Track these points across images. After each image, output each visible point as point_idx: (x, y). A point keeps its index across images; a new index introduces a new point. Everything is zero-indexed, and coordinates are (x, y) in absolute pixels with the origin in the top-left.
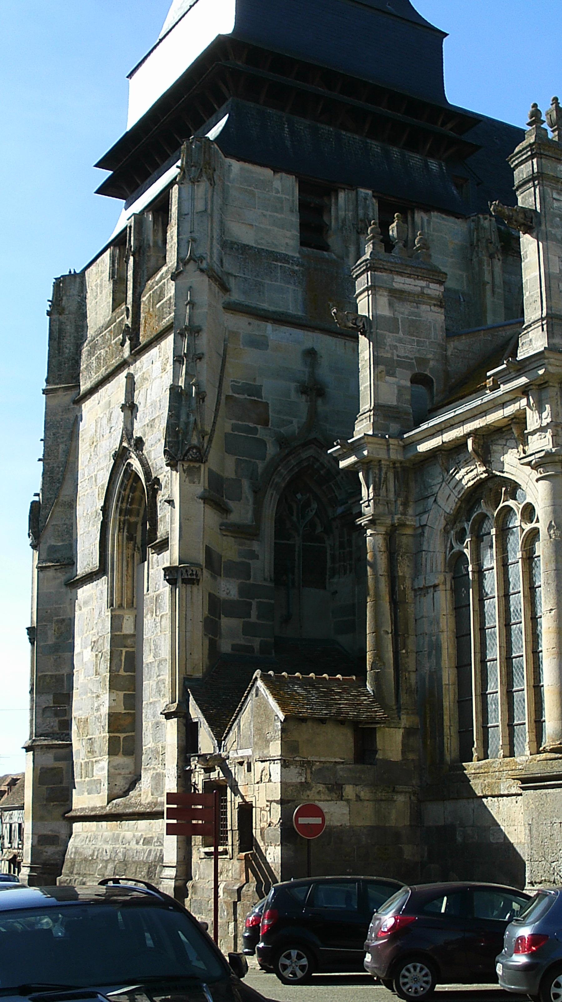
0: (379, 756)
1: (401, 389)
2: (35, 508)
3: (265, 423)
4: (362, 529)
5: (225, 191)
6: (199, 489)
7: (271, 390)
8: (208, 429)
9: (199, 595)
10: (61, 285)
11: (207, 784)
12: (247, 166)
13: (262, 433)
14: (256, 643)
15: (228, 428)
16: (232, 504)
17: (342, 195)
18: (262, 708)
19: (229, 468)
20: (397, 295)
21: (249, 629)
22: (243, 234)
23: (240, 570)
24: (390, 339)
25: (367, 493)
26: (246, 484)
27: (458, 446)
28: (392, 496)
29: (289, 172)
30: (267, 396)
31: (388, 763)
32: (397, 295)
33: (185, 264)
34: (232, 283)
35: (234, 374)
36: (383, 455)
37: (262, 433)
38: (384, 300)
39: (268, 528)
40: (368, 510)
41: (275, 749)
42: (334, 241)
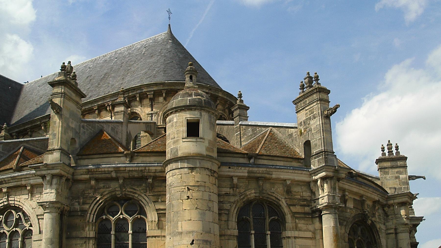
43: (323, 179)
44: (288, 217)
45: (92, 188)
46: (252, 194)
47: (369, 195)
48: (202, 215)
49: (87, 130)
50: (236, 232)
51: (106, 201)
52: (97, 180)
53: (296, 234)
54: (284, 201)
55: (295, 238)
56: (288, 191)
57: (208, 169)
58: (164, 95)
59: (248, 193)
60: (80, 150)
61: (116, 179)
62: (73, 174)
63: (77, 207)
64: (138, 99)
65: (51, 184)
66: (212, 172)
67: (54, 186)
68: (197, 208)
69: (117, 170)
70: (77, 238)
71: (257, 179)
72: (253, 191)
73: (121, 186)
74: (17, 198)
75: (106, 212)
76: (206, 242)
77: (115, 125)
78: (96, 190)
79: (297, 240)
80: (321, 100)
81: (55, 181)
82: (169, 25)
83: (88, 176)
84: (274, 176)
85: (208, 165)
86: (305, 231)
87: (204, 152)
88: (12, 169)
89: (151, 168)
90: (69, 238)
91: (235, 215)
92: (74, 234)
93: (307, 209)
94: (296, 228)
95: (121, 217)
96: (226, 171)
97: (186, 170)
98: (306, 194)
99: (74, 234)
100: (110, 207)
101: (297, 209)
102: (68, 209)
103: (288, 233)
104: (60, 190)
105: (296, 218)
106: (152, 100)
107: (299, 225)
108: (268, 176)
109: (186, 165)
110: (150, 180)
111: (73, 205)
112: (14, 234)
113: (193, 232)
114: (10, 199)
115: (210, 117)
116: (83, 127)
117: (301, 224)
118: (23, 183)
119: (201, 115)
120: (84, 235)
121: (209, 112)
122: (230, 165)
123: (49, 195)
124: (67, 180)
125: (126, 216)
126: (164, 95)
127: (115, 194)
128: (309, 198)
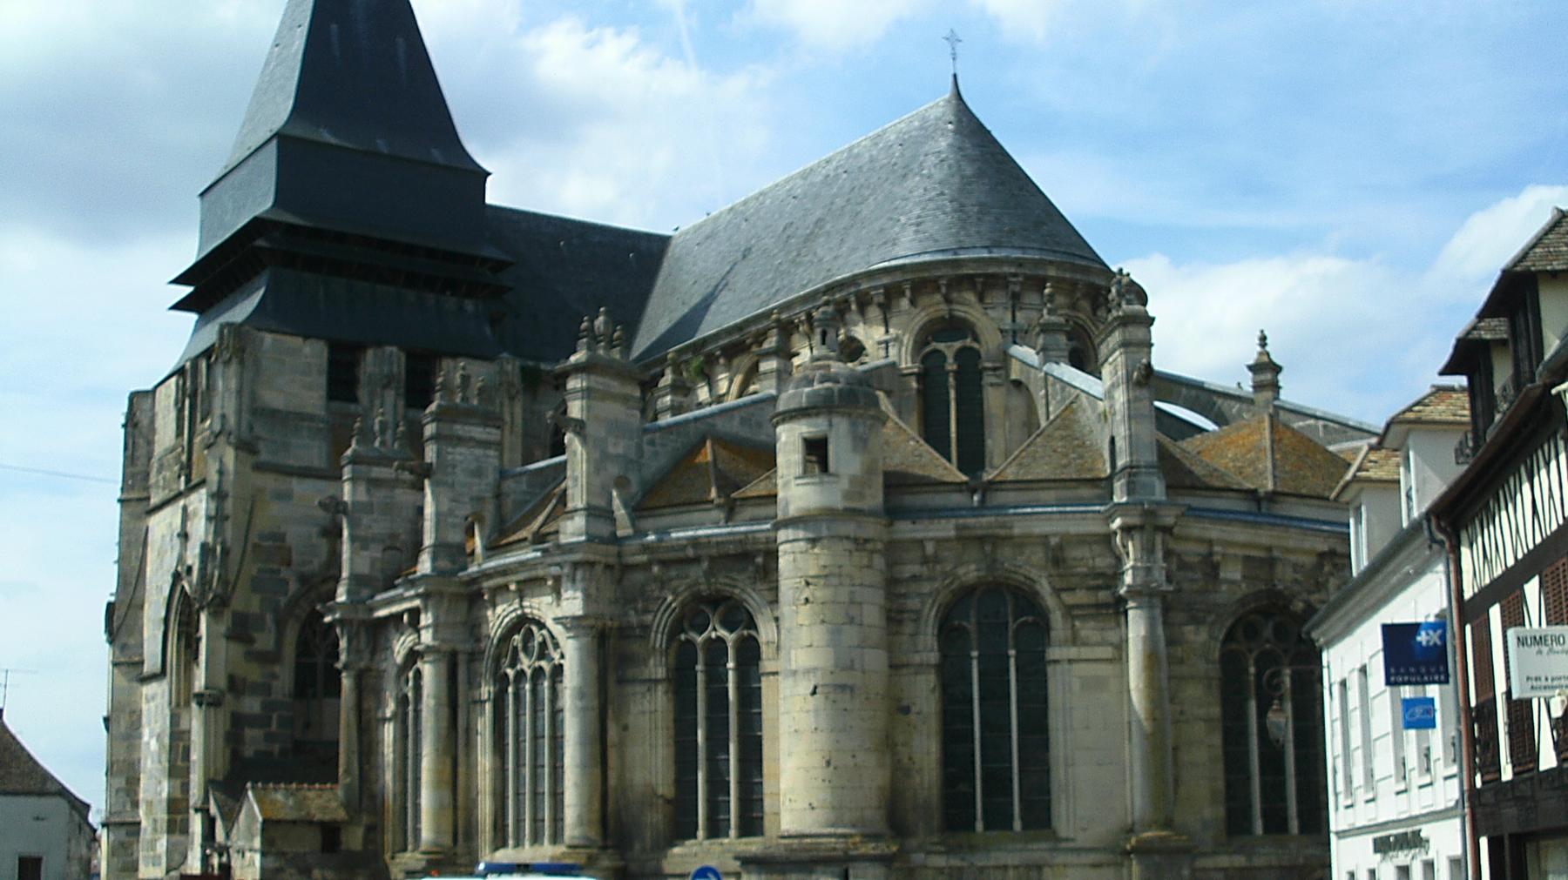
0: (343, 847)
1: (373, 561)
2: (111, 608)
3: (289, 564)
4: (339, 672)
5: (257, 363)
6: (222, 628)
7: (297, 535)
8: (232, 578)
9: (222, 718)
10: (135, 397)
11: (221, 865)
12: (279, 337)
13: (285, 573)
14: (276, 748)
15: (254, 571)
16: (256, 635)
17: (370, 354)
18: (252, 810)
19: (254, 604)
20: (374, 483)
21: (269, 737)
22: (273, 398)
23: (264, 689)
24: (366, 520)
25: (343, 644)
26: (269, 618)
27: (399, 616)
28: (362, 645)
29: (318, 337)
30: (290, 540)
31: (351, 853)
32: (374, 483)
33: (217, 436)
34: (261, 445)
35: (262, 524)
36: (352, 616)
37: (285, 573)
38: (362, 488)
39: (289, 651)
40: (343, 657)
41: (257, 843)
42: (363, 393)
43: (1127, 530)
44: (1057, 619)
45: (655, 579)
46: (970, 572)
47: (1291, 544)
48: (835, 635)
49: (663, 445)
50: (934, 657)
51: (683, 605)
52: (664, 563)
53: (1072, 652)
54: (1044, 582)
55: (1070, 661)
56: (1057, 558)
57: (848, 538)
58: (908, 293)
59: (961, 571)
60: (644, 496)
61: (696, 560)
62: (619, 555)
63: (633, 619)
64: (854, 307)
65: (574, 581)
66: (860, 543)
67: (579, 585)
68: (823, 622)
69: (695, 542)
70: (634, 681)
71: (981, 540)
72: (973, 567)
73: (709, 574)
74: (535, 601)
75: (686, 625)
76: (842, 688)
77: (751, 410)
78: (663, 583)
79: (1075, 666)
80: (1125, 344)
81: (579, 575)
82: (955, 76)
83: (644, 558)
84: (1016, 531)
85: (849, 528)
86: (1099, 644)
87: (838, 502)
88: (525, 539)
89: (758, 535)
90: (622, 681)
91: (931, 621)
92: (630, 673)
93: (1103, 596)
94: (1075, 640)
95: (713, 635)
96: (906, 530)
97: (802, 544)
98: (1103, 563)
99: (630, 673)
100: (694, 614)
101: (1081, 597)
102: (616, 624)
103: (1053, 653)
104: (593, 591)
105: (1078, 617)
106: (886, 307)
107: (1083, 633)
108: (1002, 532)
109: (801, 534)
110: (759, 560)
111: (626, 614)
112: (538, 672)
113: (815, 669)
114: (526, 603)
115: (853, 424)
116: (652, 443)
117: (1088, 630)
118: (540, 572)
119: (830, 425)
120: (646, 676)
121: (850, 415)
122: (915, 514)
123: (573, 603)
124: (608, 567)
125: (722, 633)
126: (908, 293)
127: (699, 591)
128: (1110, 572)
